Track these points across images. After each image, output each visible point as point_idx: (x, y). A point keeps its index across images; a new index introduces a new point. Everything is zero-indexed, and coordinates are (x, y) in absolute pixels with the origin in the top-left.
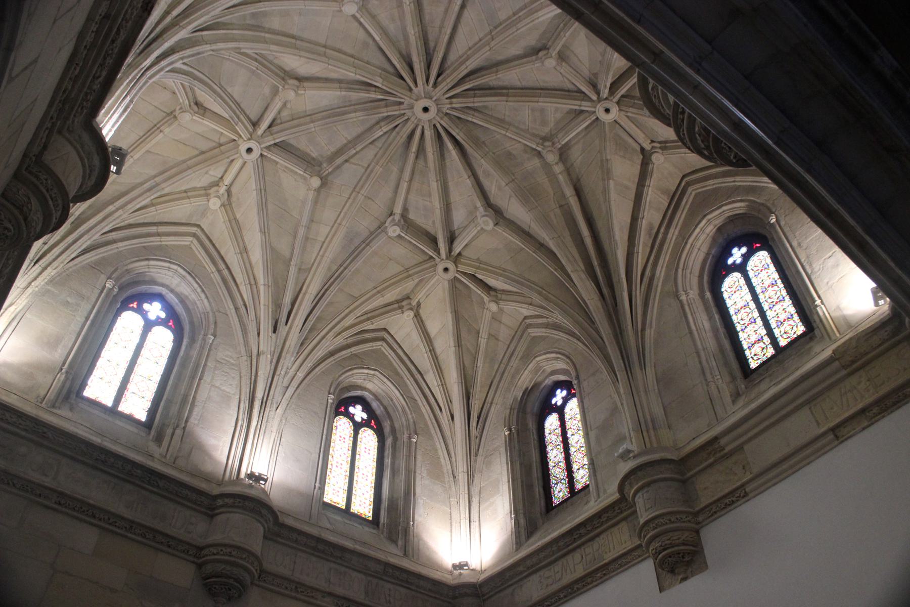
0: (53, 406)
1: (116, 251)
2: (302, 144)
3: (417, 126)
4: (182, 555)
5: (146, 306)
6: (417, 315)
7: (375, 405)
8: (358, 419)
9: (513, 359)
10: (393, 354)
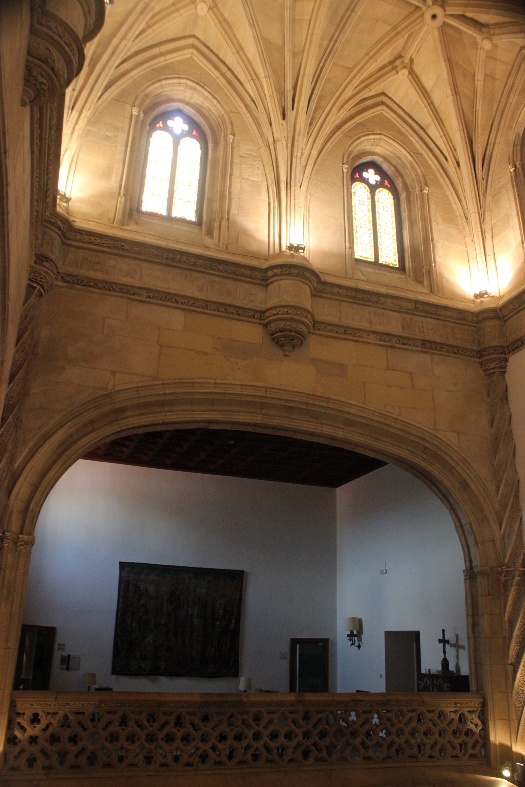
0: (123, 224)
1: (131, 80)
4: (250, 320)
5: (170, 123)
6: (412, 72)
7: (385, 166)
8: (372, 182)
9: (512, 95)
10: (394, 116)
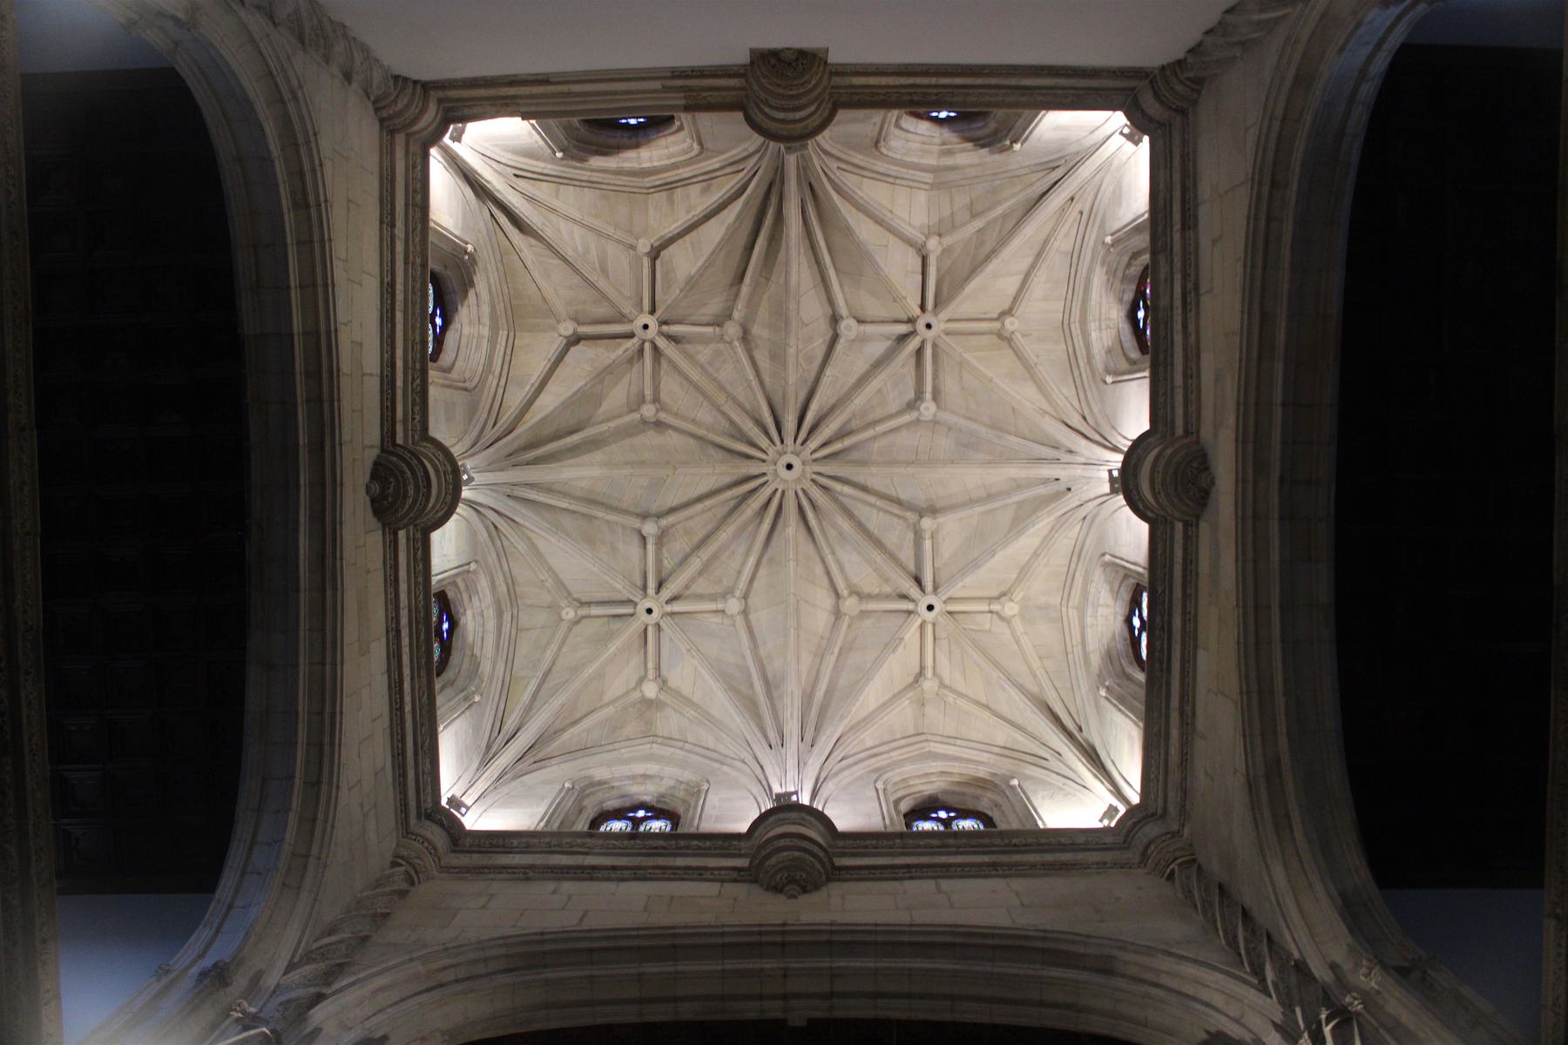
2: (907, 555)
3: (815, 460)
6: (1008, 312)
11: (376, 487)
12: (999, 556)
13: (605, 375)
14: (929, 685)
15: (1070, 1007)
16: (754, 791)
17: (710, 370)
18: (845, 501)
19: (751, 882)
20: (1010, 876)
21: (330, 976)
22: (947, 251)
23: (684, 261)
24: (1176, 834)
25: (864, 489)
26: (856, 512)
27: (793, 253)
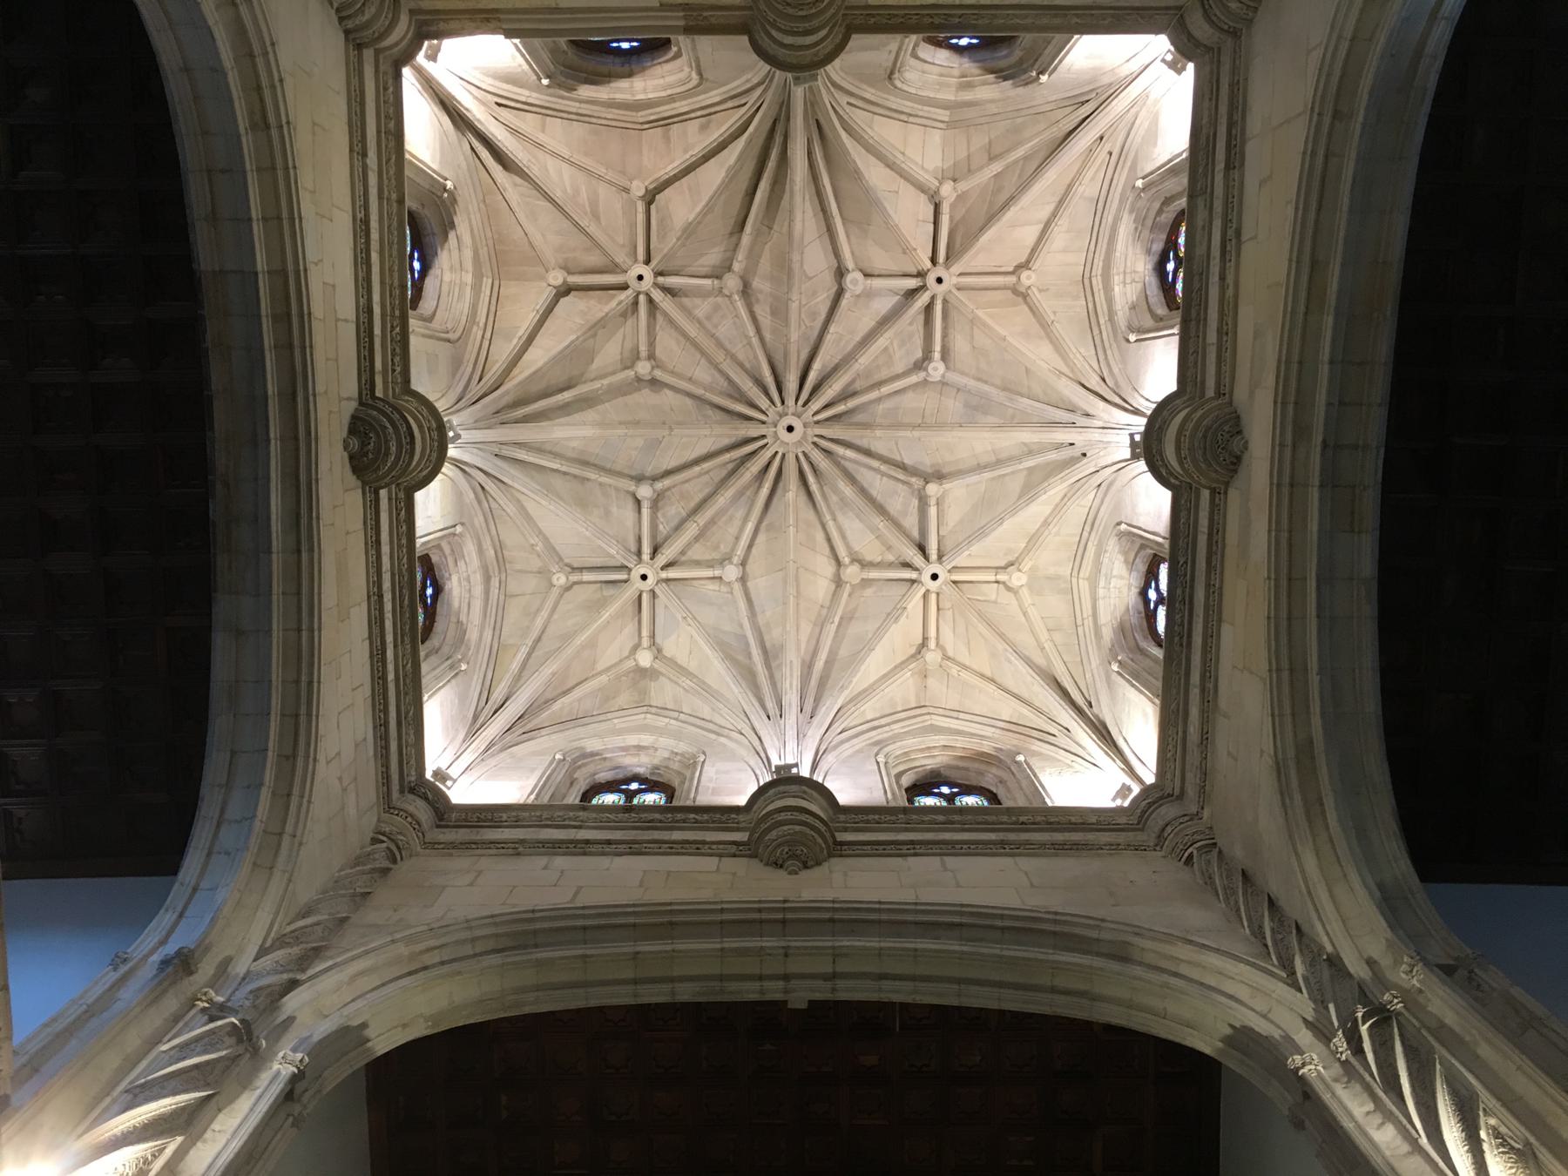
2: (911, 522)
3: (817, 422)
6: (1025, 266)
11: (355, 443)
12: (1008, 524)
13: (597, 328)
14: (932, 657)
15: (1082, 994)
16: (752, 763)
17: (709, 325)
18: (848, 465)
19: (750, 856)
20: (1020, 855)
21: (303, 962)
22: (961, 198)
23: (681, 207)
24: (1197, 816)
25: (868, 453)
26: (858, 477)
27: (798, 199)
